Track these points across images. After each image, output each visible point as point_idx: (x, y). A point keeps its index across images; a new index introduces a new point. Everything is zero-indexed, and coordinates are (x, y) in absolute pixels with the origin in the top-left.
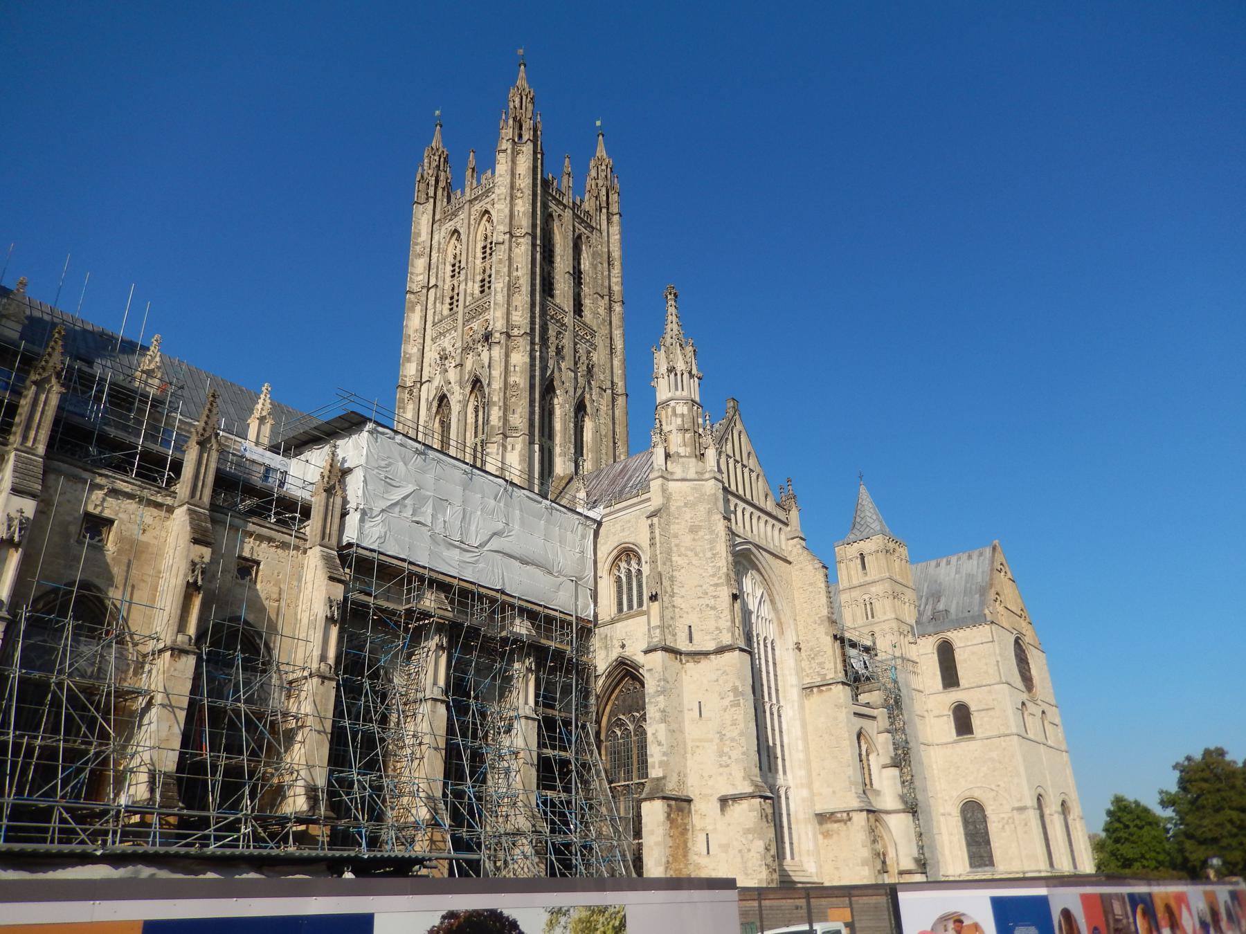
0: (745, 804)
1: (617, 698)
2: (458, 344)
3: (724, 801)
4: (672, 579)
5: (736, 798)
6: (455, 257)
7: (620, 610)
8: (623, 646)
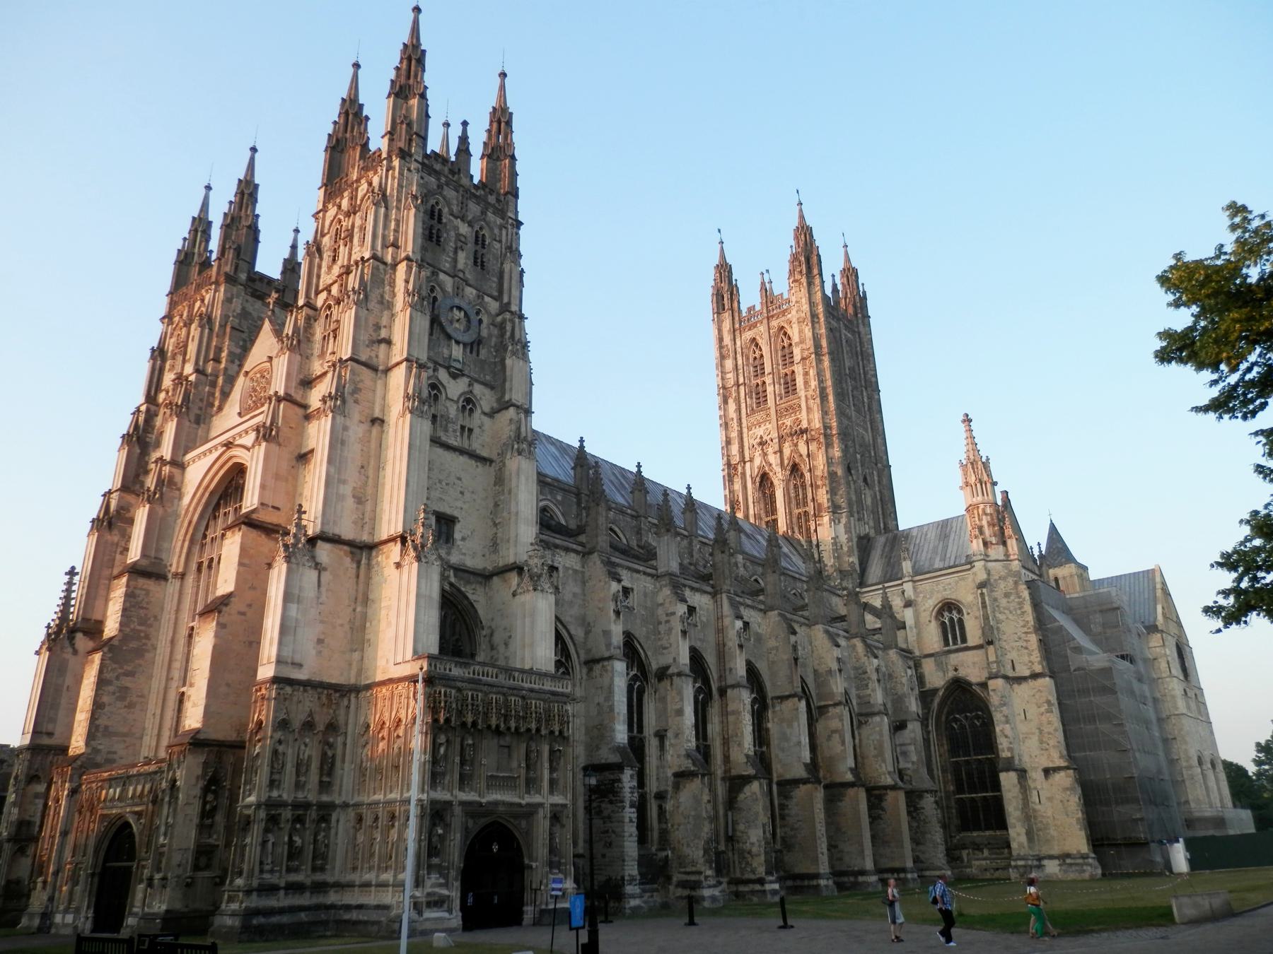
0: (1062, 774)
1: (952, 703)
2: (775, 435)
3: (1047, 772)
4: (998, 628)
5: (1057, 769)
6: (755, 358)
7: (947, 644)
8: (956, 670)
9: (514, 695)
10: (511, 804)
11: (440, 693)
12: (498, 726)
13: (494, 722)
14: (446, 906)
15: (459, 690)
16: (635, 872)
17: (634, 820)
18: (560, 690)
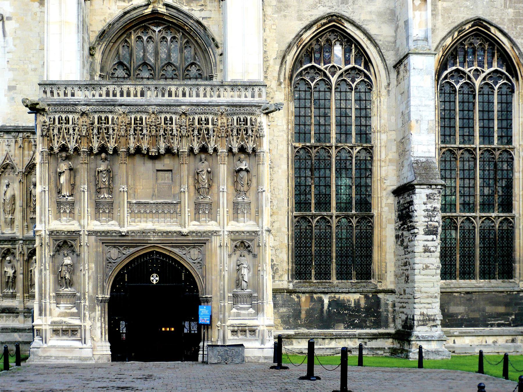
9: (161, 112)
10: (167, 233)
11: (54, 119)
12: (138, 150)
13: (132, 145)
14: (79, 335)
15: (83, 114)
16: (435, 310)
17: (432, 249)
18: (249, 100)
